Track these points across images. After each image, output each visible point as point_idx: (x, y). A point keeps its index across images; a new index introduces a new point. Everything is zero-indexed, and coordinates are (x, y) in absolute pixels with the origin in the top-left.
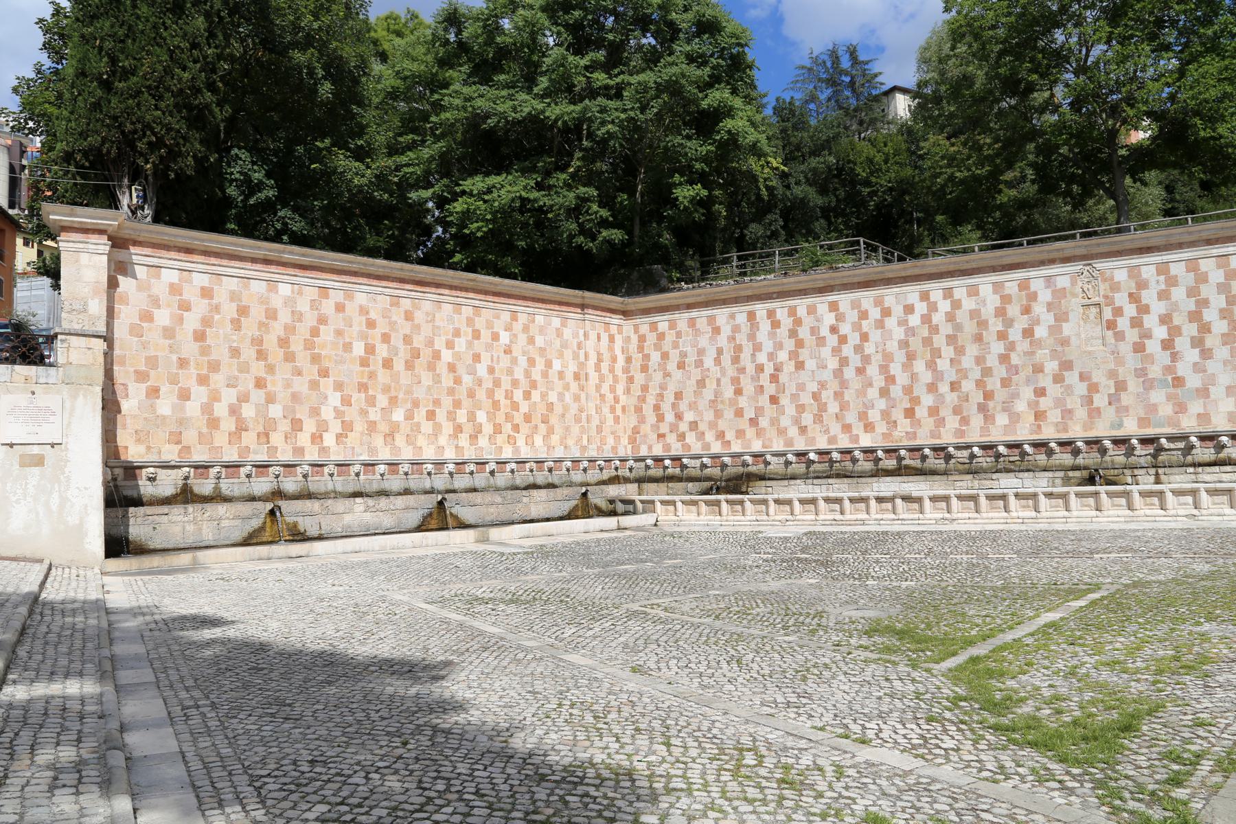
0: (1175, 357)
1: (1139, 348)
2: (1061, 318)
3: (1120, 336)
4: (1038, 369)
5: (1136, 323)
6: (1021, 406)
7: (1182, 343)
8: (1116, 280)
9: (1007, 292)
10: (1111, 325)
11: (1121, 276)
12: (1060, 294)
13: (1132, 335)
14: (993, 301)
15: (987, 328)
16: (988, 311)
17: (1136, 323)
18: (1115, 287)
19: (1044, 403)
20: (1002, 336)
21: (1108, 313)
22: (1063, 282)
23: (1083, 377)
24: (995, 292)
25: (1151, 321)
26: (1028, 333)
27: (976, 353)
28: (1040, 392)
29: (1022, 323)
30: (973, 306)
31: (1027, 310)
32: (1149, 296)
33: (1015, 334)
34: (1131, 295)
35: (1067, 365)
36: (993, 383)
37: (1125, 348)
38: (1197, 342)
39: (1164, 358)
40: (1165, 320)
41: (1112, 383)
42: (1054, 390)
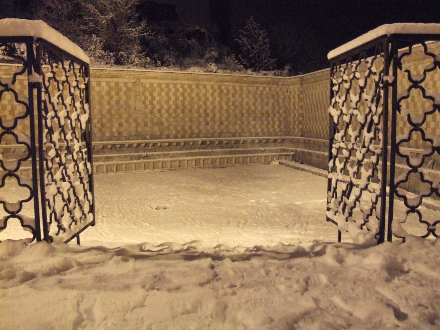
0: (161, 115)
1: (152, 112)
2: (129, 97)
3: (146, 107)
4: (121, 117)
5: (151, 103)
6: (114, 130)
7: (163, 111)
8: (146, 86)
9: (111, 86)
10: (144, 103)
11: (148, 85)
12: (128, 89)
13: (150, 107)
14: (106, 89)
15: (103, 99)
16: (104, 93)
17: (151, 103)
18: (145, 89)
19: (122, 129)
20: (109, 103)
21: (143, 98)
22: (130, 85)
23: (135, 120)
24: (107, 85)
25: (155, 102)
26: (118, 102)
27: (99, 108)
28: (121, 125)
29: (115, 98)
30: (98, 90)
31: (117, 94)
32: (155, 94)
33: (113, 103)
34: (150, 93)
35: (130, 116)
36: (105, 121)
37: (148, 111)
38: (167, 111)
39: (158, 115)
40: (159, 103)
41: (143, 123)
42: (125, 125)
